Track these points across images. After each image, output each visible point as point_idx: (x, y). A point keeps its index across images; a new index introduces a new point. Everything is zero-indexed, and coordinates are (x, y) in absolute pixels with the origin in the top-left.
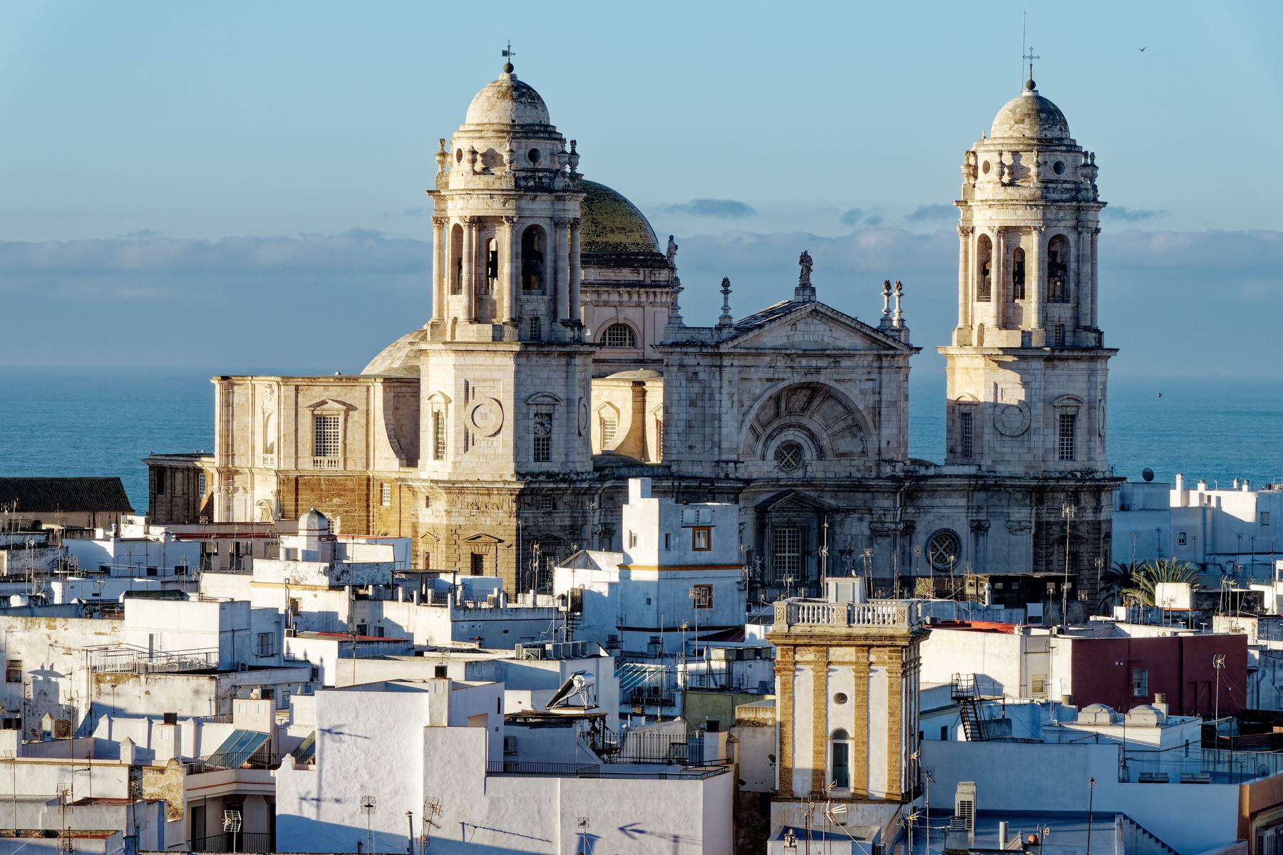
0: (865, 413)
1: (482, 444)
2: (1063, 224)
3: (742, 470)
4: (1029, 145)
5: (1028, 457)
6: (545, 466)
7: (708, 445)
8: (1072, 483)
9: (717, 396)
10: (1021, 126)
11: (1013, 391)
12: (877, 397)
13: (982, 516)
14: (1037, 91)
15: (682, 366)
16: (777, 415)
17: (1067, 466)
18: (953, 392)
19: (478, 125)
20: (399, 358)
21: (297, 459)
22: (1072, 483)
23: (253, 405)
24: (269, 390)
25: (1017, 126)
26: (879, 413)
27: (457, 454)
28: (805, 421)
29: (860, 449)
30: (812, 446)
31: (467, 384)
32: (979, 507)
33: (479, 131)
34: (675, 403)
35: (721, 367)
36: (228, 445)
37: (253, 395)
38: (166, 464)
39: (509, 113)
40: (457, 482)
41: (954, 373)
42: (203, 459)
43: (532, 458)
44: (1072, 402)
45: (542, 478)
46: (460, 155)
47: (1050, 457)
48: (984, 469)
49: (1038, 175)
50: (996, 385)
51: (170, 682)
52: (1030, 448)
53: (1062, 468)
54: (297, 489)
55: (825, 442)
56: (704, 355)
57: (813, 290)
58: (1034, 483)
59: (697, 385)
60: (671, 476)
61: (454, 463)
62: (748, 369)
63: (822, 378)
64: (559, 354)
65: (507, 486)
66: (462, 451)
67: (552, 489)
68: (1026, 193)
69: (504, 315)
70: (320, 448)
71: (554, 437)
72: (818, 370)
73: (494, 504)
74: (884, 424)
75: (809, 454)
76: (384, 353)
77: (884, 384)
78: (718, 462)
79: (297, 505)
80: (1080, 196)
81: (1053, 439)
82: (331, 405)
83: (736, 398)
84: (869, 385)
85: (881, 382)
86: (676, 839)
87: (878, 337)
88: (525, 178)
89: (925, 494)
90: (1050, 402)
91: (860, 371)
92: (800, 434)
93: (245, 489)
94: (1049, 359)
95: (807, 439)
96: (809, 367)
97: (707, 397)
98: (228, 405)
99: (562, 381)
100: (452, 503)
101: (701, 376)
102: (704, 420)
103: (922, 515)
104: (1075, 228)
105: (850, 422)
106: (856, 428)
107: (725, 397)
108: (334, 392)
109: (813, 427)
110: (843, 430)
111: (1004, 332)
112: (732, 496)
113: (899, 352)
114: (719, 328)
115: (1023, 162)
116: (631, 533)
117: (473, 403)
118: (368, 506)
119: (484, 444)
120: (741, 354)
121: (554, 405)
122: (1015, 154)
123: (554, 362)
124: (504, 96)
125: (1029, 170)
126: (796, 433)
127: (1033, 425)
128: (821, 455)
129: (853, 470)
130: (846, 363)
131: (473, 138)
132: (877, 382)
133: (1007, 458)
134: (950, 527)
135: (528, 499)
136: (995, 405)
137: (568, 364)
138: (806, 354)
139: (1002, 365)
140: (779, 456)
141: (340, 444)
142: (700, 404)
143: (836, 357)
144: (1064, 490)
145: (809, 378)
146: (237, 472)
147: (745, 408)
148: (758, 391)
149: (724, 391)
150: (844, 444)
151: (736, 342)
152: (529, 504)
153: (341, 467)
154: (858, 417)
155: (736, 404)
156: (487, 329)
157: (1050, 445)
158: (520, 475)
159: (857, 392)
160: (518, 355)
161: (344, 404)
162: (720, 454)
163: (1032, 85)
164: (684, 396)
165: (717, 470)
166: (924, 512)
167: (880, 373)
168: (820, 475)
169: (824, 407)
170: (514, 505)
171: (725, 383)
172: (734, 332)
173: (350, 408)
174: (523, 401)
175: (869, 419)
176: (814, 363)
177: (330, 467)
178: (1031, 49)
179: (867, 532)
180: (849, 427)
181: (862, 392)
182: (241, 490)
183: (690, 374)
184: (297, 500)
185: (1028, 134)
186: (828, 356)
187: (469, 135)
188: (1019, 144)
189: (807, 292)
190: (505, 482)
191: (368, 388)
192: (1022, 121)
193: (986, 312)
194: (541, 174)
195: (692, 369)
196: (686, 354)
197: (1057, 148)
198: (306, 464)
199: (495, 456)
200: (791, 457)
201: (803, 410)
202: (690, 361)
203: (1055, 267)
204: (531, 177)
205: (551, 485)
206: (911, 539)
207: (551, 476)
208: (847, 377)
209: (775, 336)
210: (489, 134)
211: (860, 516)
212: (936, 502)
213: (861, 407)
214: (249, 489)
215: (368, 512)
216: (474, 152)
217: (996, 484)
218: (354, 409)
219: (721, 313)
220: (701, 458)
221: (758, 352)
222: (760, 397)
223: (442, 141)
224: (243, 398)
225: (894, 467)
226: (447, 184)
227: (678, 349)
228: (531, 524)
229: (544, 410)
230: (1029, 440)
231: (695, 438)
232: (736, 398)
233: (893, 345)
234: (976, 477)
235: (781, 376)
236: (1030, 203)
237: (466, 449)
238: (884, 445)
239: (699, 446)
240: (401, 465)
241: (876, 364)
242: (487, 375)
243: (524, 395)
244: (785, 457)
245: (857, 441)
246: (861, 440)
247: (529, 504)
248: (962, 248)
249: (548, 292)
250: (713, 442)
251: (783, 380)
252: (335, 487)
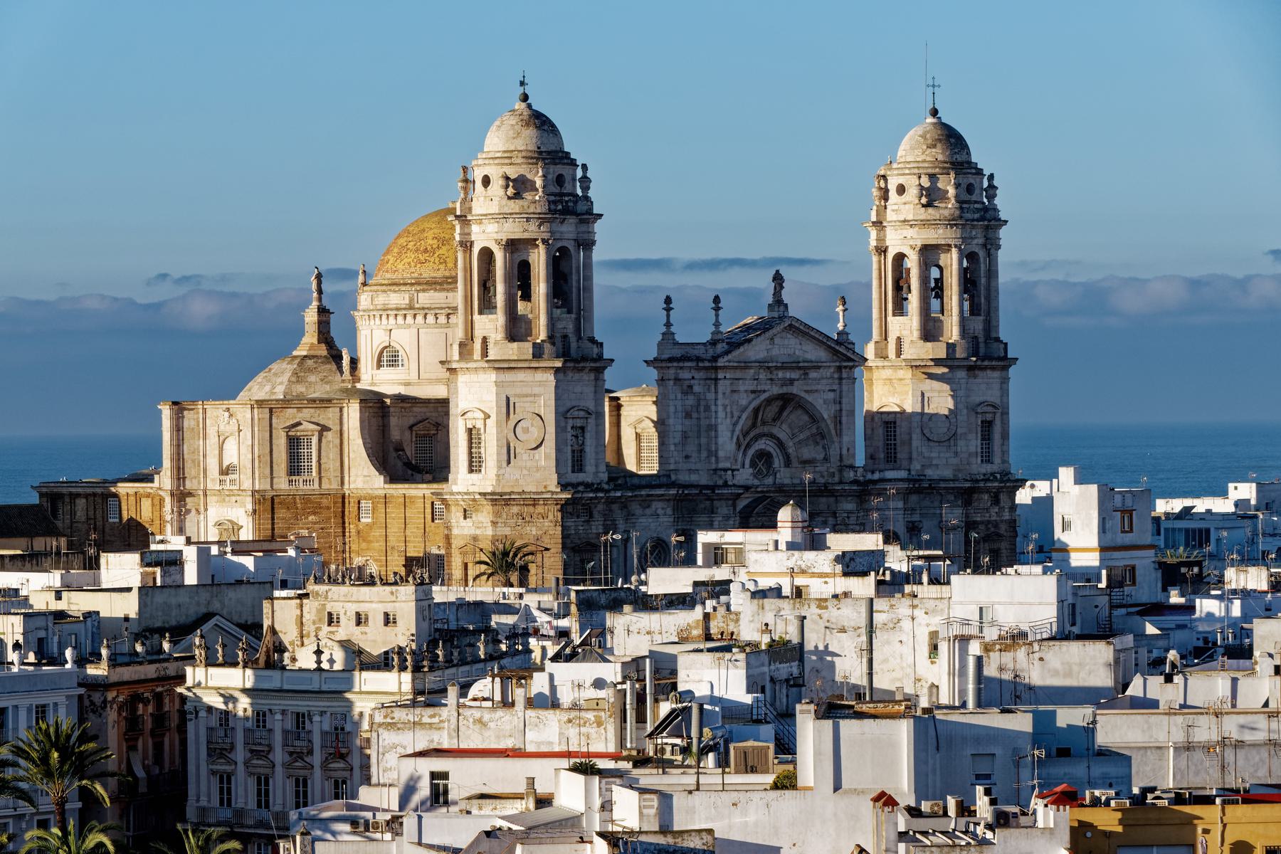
0: (829, 422)
1: (524, 457)
2: (975, 241)
3: (738, 478)
4: (944, 168)
5: (955, 461)
6: (581, 477)
7: (704, 454)
8: (996, 484)
9: (713, 408)
10: (934, 150)
11: (941, 401)
13: (916, 518)
14: (940, 118)
15: (677, 380)
16: (754, 425)
17: (988, 468)
18: (871, 401)
19: (505, 152)
20: (281, 383)
21: (272, 479)
22: (996, 484)
23: (205, 428)
24: (227, 414)
25: (929, 150)
26: (840, 422)
27: (500, 467)
28: (775, 431)
29: (822, 456)
31: (508, 399)
32: (913, 509)
33: (508, 157)
34: (672, 415)
35: (716, 379)
36: (179, 468)
37: (204, 419)
38: (65, 491)
39: (534, 140)
40: (505, 494)
41: (871, 384)
42: (119, 485)
43: (570, 469)
44: (990, 409)
45: (581, 488)
46: (486, 181)
47: (973, 460)
48: (913, 473)
49: (957, 196)
50: (923, 394)
51: (1064, 649)
52: (956, 453)
53: (983, 471)
54: (273, 509)
56: (698, 369)
57: (786, 306)
58: (968, 485)
59: (691, 397)
60: (673, 485)
61: (498, 476)
63: (795, 389)
64: (590, 370)
65: (554, 496)
66: (505, 464)
67: (591, 499)
68: (946, 213)
69: (541, 334)
70: (295, 468)
71: (587, 449)
72: (791, 382)
73: (539, 514)
74: (844, 432)
75: (777, 462)
76: (259, 378)
77: (844, 394)
78: (715, 470)
79: (273, 524)
80: (988, 216)
81: (975, 443)
82: (306, 426)
83: (728, 409)
84: (831, 395)
85: (841, 392)
86: (420, 844)
87: (841, 350)
88: (555, 202)
90: (974, 409)
91: (824, 382)
92: (771, 443)
93: (197, 510)
94: (971, 369)
96: (784, 379)
97: (702, 409)
98: (178, 429)
99: (591, 396)
100: (497, 514)
101: (697, 389)
102: (699, 431)
104: (984, 245)
105: (814, 431)
106: (820, 436)
107: (720, 408)
108: (307, 413)
109: (782, 436)
110: (808, 438)
111: (929, 344)
112: (730, 502)
114: (713, 343)
115: (940, 185)
116: (1063, 518)
117: (514, 419)
118: (344, 523)
119: (525, 457)
120: (736, 368)
121: (587, 418)
122: (932, 177)
123: (586, 377)
124: (528, 125)
125: (948, 191)
126: (768, 442)
127: (959, 431)
128: (788, 463)
129: (818, 476)
130: (813, 374)
131: (503, 164)
132: (838, 392)
133: (934, 462)
135: (570, 509)
136: (922, 414)
137: (597, 379)
138: (783, 367)
139: (931, 376)
140: (753, 464)
141: (314, 464)
142: (695, 415)
143: (804, 368)
144: (988, 491)
145: (785, 390)
146: (190, 494)
147: (735, 419)
148: (744, 402)
149: (719, 402)
150: (807, 453)
151: (730, 357)
152: (571, 514)
153: (316, 486)
154: (823, 425)
155: (729, 415)
156: (527, 348)
157: (973, 449)
158: (564, 486)
159: (822, 403)
160: (557, 370)
161: (318, 424)
162: (717, 462)
163: (934, 112)
164: (680, 408)
165: (716, 478)
167: (840, 384)
168: (787, 481)
169: (793, 417)
170: (559, 514)
171: (720, 396)
172: (726, 347)
173: (324, 429)
174: (562, 415)
175: (832, 426)
176: (788, 375)
177: (307, 484)
178: (933, 78)
180: (812, 435)
181: (825, 402)
182: (193, 512)
183: (685, 388)
184: (273, 519)
185: (940, 157)
186: (800, 368)
187: (497, 161)
188: (936, 167)
189: (782, 308)
190: (553, 493)
191: (341, 409)
192: (934, 146)
193: (906, 326)
194: (567, 199)
195: (687, 383)
196: (681, 368)
197: (969, 171)
198: (282, 484)
199: (538, 469)
201: (774, 420)
202: (685, 375)
203: (969, 283)
204: (559, 201)
205: (591, 495)
207: (588, 486)
208: (814, 388)
209: (757, 350)
210: (520, 161)
213: (826, 416)
214: (202, 509)
215: (344, 528)
216: (507, 178)
217: (930, 487)
218: (329, 429)
219: (713, 329)
220: (698, 466)
221: (745, 365)
222: (746, 408)
223: (465, 169)
224: (193, 423)
225: (856, 472)
226: (470, 209)
227: (675, 364)
228: (573, 532)
229: (579, 423)
230: (955, 445)
231: (691, 448)
232: (728, 409)
233: (852, 357)
234: (908, 480)
236: (951, 223)
237: (509, 462)
238: (844, 452)
239: (695, 455)
240: (385, 482)
241: (836, 376)
242: (527, 390)
243: (562, 409)
245: (819, 448)
246: (824, 448)
247: (571, 514)
248: (875, 266)
249: (574, 310)
250: (709, 451)
251: (764, 391)
252: (310, 504)
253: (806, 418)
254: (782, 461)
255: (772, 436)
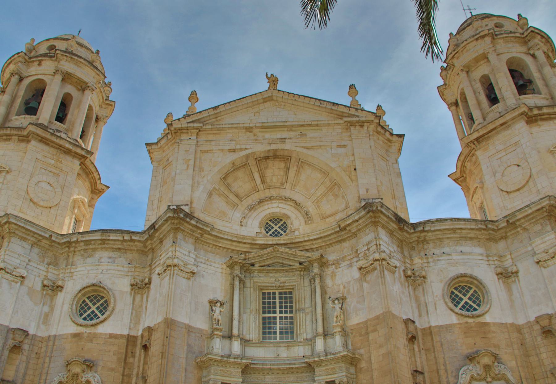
12: (351, 158)
28: (287, 193)
30: (299, 215)
55: (312, 210)
62: (208, 143)
72: (283, 140)
84: (341, 150)
89: (431, 245)
92: (285, 206)
95: (293, 209)
103: (432, 264)
113: (364, 119)
126: (281, 205)
128: (308, 218)
134: (469, 272)
145: (274, 147)
150: (327, 207)
166: (434, 261)
169: (303, 177)
179: (356, 274)
200: (276, 225)
206: (423, 288)
211: (349, 262)
212: (446, 250)
213: (333, 165)
230: (535, 185)
232: (192, 162)
233: (356, 114)
235: (243, 147)
244: (276, 230)
246: (343, 197)
251: (246, 149)
253: (319, 175)
254: (303, 221)
255: (286, 199)
